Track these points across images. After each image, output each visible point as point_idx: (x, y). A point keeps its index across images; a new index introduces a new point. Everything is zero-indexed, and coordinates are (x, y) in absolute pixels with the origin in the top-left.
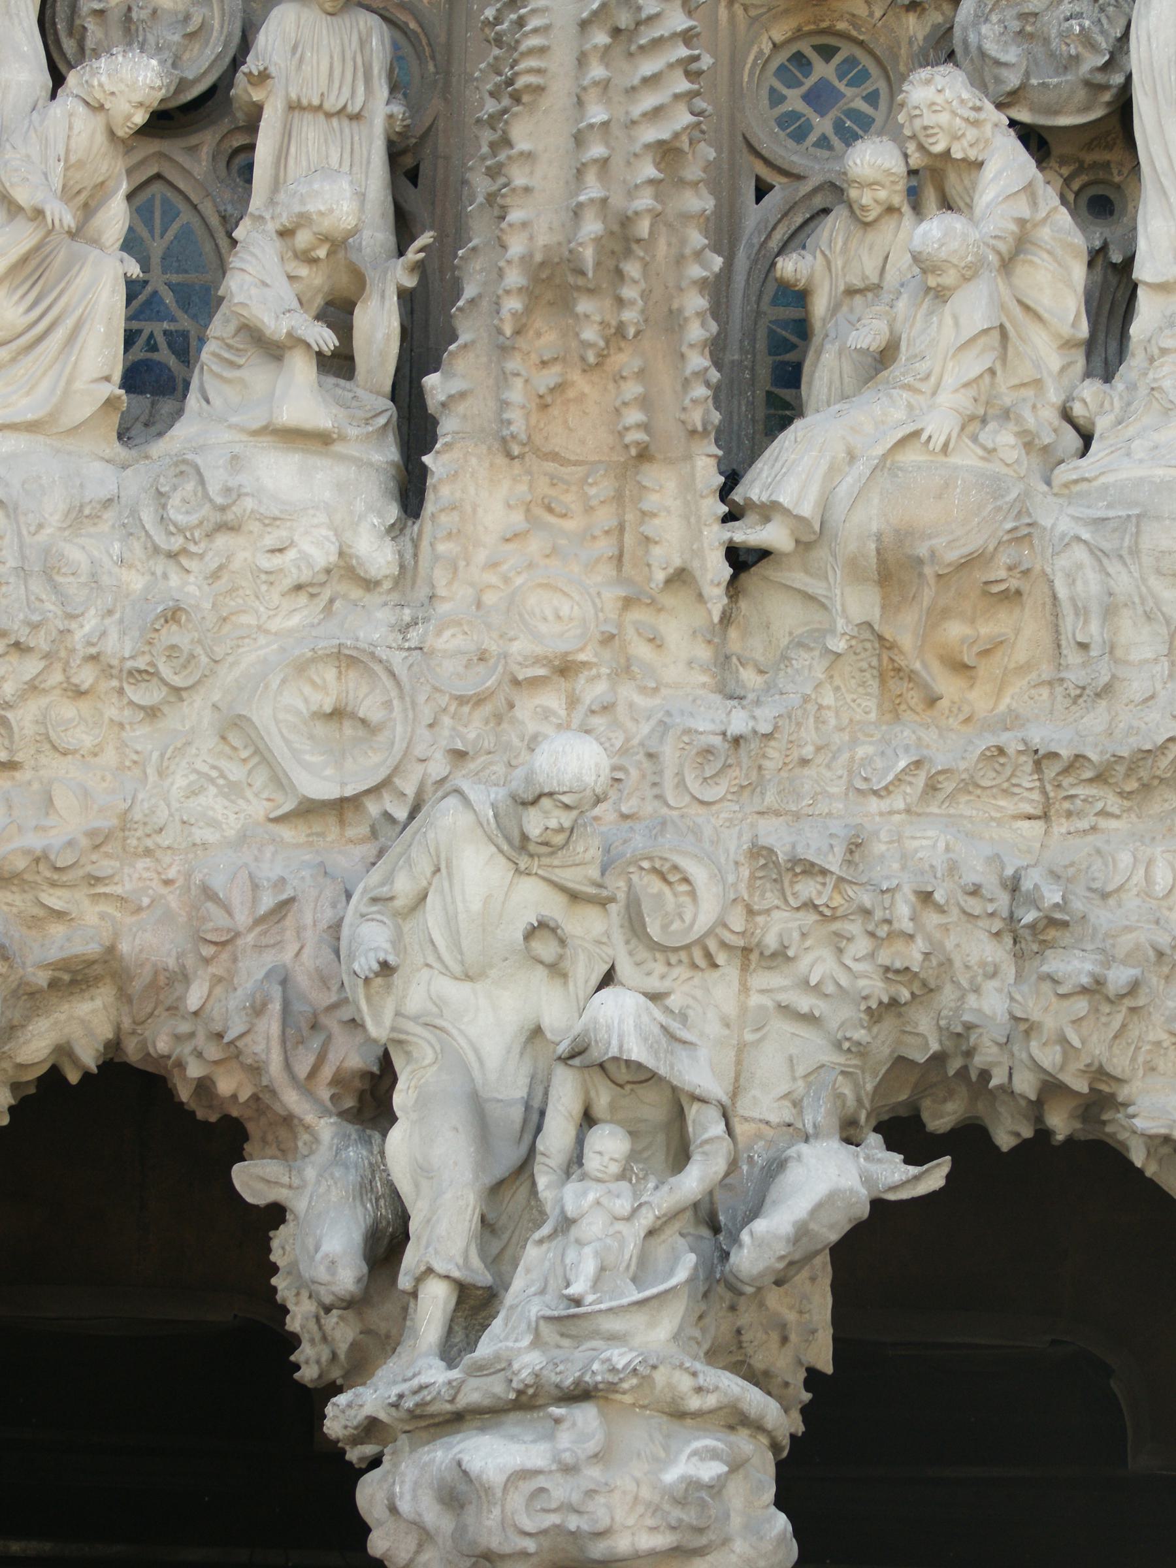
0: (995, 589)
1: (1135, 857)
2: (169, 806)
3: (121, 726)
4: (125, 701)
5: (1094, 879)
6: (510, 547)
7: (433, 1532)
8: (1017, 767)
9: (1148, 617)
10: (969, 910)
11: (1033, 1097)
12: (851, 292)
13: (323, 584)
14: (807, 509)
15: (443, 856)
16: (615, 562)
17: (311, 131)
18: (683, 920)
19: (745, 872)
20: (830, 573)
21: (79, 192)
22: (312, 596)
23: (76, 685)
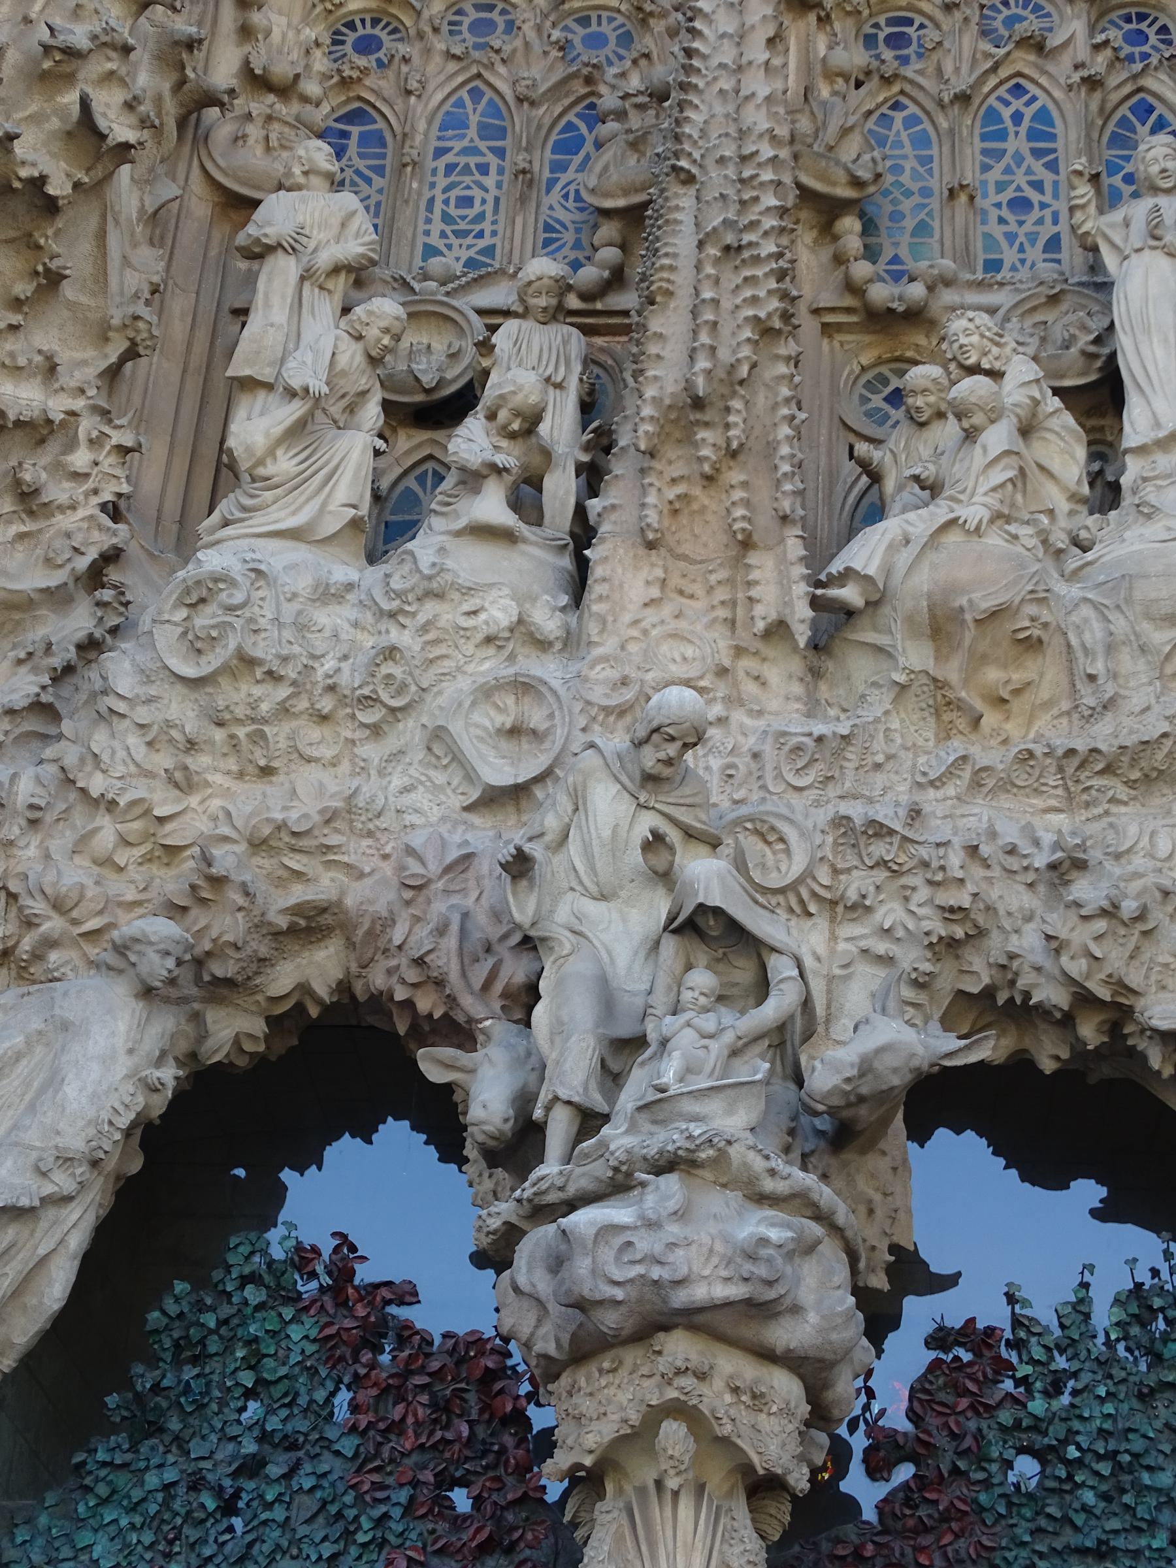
0: (1021, 636)
3: (353, 742)
6: (649, 611)
7: (544, 1299)
9: (1143, 649)
11: (1066, 1008)
13: (508, 639)
14: (871, 571)
18: (779, 869)
19: (830, 839)
21: (343, 396)
22: (500, 647)
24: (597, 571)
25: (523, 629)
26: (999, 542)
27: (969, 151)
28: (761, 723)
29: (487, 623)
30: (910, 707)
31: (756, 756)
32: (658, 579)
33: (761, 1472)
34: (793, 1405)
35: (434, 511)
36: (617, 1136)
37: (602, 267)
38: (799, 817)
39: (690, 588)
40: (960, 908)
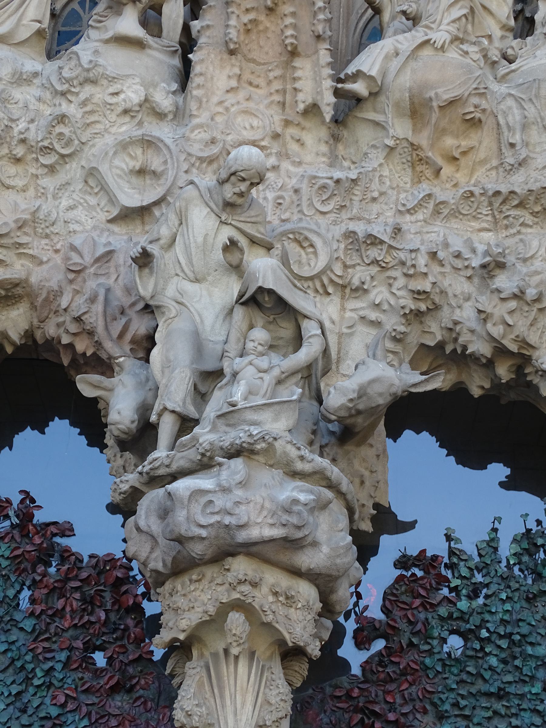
0: (468, 117)
1: (540, 243)
2: (58, 213)
3: (37, 176)
4: (39, 164)
5: (519, 254)
6: (230, 95)
7: (156, 536)
8: (480, 203)
10: (456, 266)
11: (489, 356)
13: (138, 111)
14: (373, 73)
15: (183, 214)
16: (281, 106)
19: (342, 246)
20: (386, 108)
22: (133, 117)
23: (15, 155)
24: (197, 69)
25: (147, 105)
26: (456, 55)
28: (300, 170)
29: (124, 100)
30: (396, 161)
31: (296, 191)
32: (235, 74)
33: (291, 644)
34: (311, 603)
35: (91, 26)
36: (204, 434)
38: (323, 231)
39: (256, 81)
40: (424, 292)
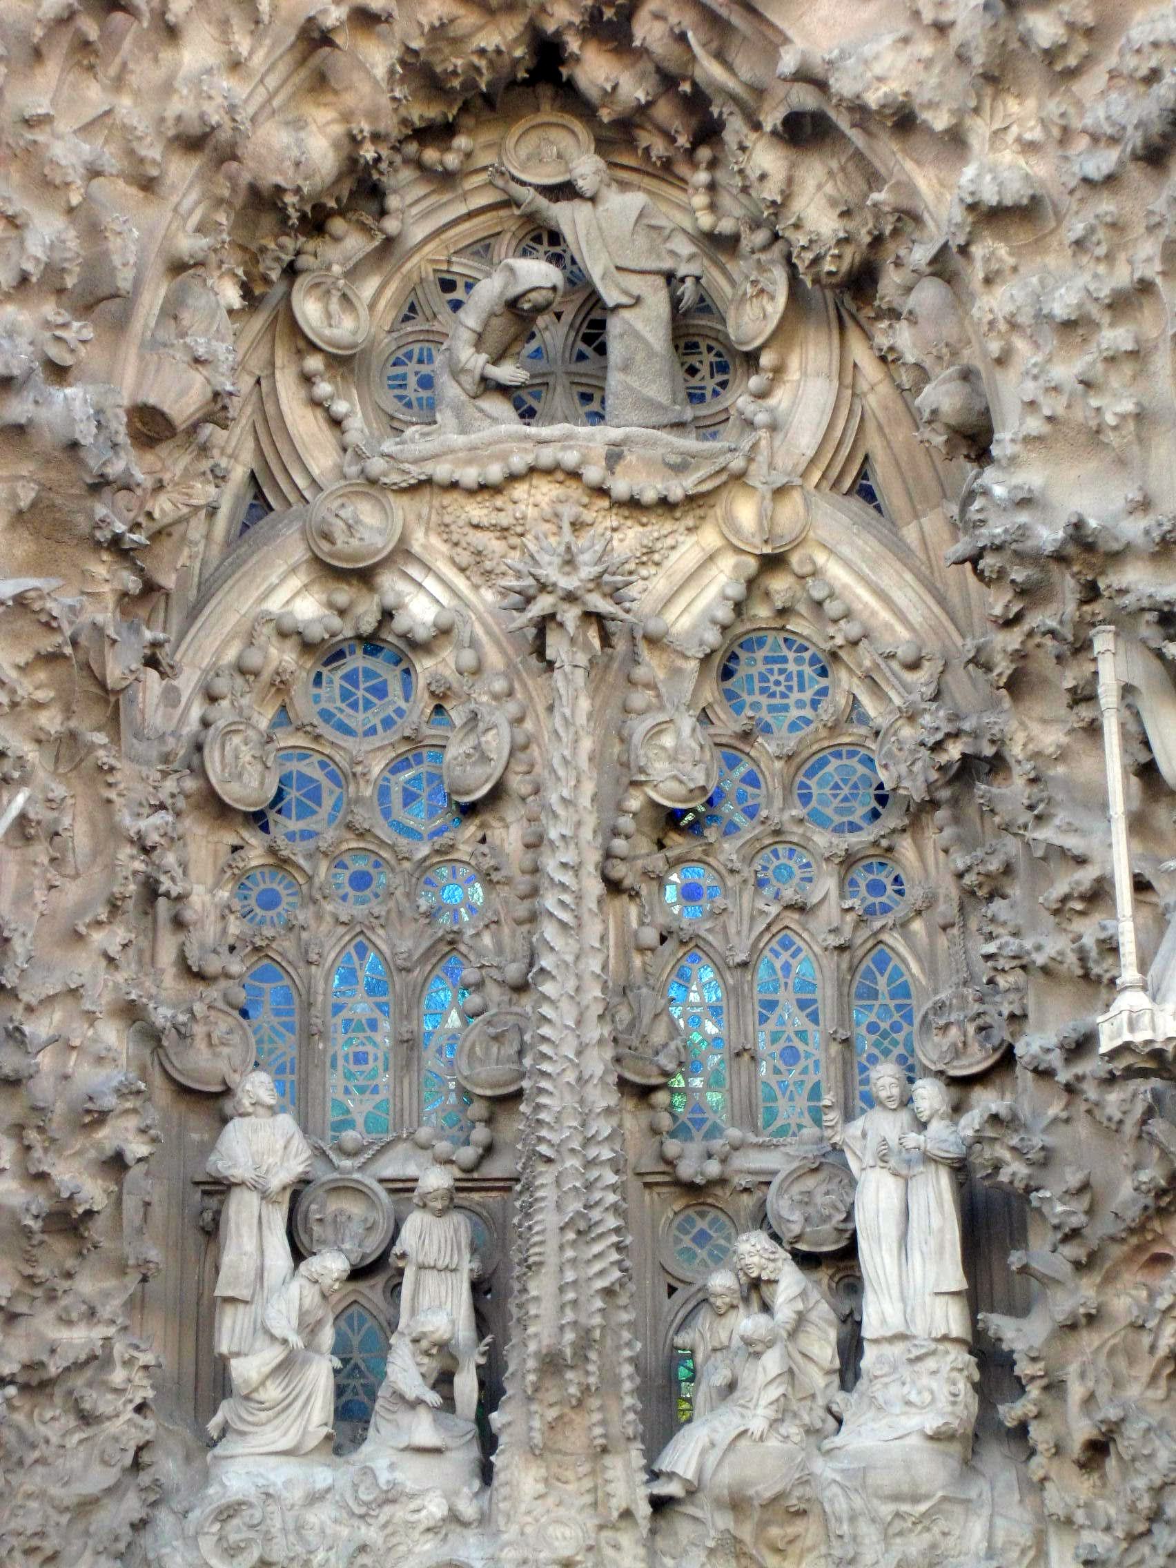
6: (539, 1502)
12: (715, 1350)
14: (690, 1475)
17: (430, 1278)
24: (500, 1478)
27: (749, 1007)
37: (477, 1145)
